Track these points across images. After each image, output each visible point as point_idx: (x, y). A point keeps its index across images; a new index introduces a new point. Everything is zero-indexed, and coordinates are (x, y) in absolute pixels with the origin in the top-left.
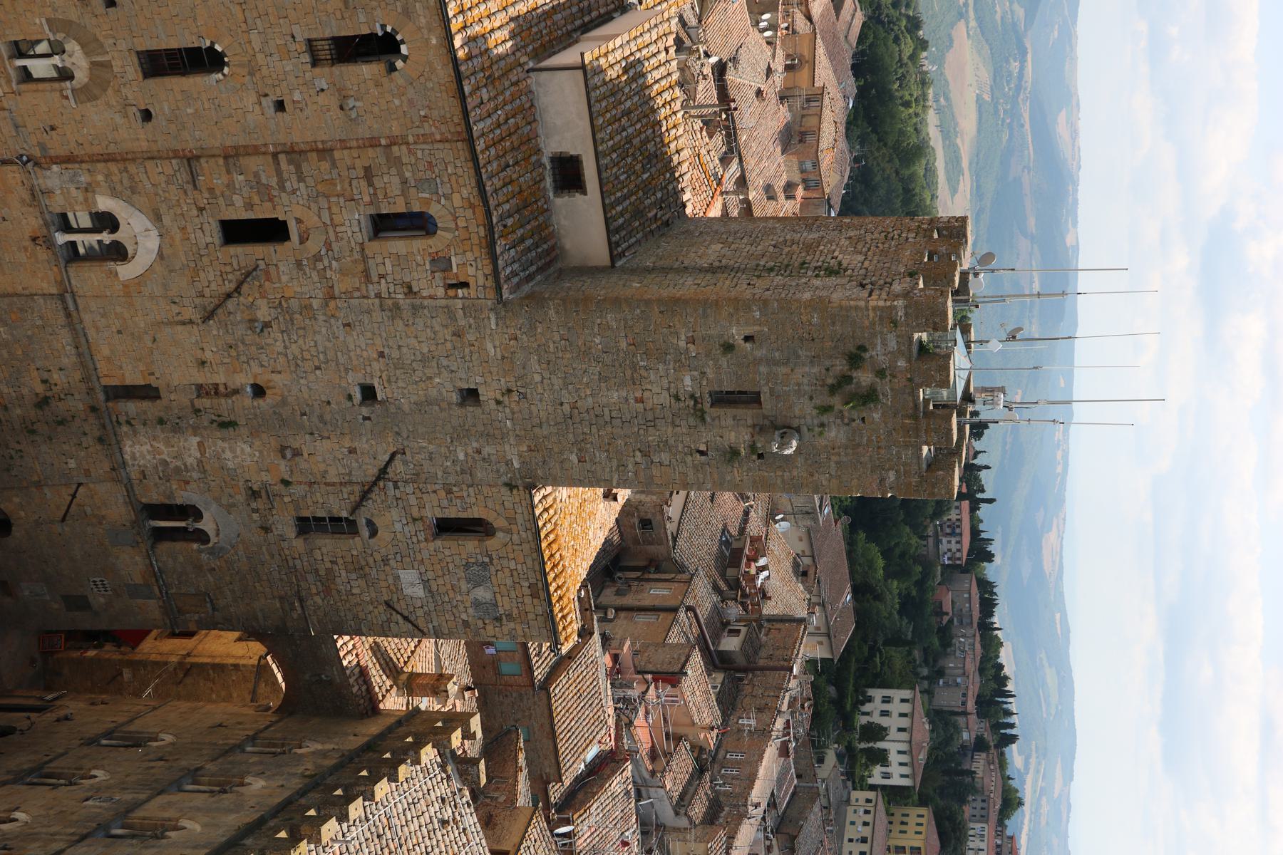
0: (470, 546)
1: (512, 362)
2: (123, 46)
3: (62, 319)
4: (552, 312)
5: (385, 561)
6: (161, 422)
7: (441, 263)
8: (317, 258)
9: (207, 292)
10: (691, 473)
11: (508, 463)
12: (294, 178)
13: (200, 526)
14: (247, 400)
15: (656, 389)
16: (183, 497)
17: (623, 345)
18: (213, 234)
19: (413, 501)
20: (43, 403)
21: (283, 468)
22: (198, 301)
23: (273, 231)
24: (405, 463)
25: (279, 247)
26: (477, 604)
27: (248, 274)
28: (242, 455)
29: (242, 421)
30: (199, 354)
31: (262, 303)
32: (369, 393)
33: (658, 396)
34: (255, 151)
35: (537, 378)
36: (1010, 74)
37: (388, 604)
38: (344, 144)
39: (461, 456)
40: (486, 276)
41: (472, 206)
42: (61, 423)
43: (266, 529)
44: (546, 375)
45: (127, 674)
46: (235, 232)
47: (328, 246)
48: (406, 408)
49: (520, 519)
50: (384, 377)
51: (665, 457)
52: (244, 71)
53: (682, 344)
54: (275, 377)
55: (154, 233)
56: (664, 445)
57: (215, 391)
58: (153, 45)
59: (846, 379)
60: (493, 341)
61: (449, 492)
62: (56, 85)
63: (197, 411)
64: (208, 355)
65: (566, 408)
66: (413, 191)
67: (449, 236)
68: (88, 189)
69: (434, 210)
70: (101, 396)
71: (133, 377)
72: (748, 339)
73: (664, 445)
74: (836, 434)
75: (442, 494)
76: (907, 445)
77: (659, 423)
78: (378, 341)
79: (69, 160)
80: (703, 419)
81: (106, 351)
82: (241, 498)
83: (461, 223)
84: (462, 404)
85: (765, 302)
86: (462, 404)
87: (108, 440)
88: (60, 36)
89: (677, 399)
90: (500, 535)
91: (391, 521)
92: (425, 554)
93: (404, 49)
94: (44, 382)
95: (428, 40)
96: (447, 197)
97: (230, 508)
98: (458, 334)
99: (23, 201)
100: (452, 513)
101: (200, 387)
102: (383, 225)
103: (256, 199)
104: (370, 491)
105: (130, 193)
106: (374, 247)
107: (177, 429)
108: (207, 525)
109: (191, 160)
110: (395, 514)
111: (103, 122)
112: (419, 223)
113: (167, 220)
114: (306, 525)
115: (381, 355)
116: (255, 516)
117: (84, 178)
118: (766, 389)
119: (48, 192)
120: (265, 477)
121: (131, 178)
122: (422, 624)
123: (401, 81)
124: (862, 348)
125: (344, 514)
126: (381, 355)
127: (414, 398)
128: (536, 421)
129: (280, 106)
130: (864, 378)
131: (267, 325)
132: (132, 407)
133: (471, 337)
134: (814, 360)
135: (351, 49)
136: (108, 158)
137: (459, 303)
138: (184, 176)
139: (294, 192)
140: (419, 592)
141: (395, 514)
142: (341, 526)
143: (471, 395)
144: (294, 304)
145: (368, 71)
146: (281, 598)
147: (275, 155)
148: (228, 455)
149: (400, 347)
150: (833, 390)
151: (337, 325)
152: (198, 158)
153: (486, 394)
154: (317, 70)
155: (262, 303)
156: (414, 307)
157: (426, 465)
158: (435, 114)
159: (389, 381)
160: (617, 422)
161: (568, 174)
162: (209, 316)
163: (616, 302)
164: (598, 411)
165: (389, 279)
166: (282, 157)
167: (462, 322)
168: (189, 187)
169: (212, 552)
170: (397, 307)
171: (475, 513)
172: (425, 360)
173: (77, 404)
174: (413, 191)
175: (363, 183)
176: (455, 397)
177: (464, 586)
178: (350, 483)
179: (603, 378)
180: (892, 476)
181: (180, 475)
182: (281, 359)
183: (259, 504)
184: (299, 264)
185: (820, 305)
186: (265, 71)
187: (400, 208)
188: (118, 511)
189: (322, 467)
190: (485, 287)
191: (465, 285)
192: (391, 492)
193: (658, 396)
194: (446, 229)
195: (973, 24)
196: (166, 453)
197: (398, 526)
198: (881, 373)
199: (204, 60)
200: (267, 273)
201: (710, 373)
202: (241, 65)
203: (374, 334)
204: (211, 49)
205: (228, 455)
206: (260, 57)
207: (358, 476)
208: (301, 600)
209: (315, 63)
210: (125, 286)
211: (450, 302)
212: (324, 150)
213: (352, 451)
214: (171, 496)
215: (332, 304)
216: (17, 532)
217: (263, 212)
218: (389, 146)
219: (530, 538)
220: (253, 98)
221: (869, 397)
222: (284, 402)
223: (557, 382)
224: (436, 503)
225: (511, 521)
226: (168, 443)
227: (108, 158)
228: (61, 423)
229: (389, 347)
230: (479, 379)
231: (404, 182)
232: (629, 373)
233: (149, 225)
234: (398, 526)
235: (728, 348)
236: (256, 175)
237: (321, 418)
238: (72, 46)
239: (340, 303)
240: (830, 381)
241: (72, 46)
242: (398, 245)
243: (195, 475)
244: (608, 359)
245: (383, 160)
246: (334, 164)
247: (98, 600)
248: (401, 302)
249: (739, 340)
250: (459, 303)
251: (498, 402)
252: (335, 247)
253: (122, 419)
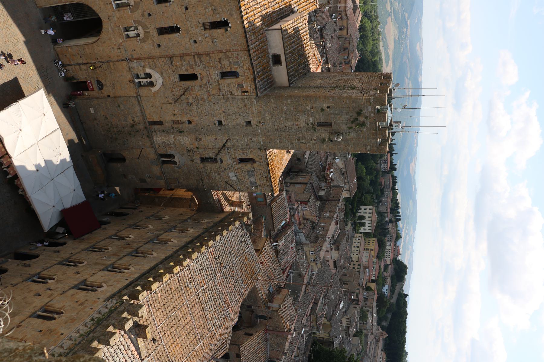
0: (249, 166)
2: (153, 27)
3: (137, 103)
4: (272, 99)
5: (225, 170)
6: (163, 131)
7: (240, 86)
8: (206, 84)
9: (175, 95)
10: (311, 146)
11: (260, 143)
12: (199, 62)
13: (174, 160)
14: (187, 124)
16: (170, 152)
17: (292, 109)
18: (177, 79)
19: (233, 153)
20: (133, 126)
21: (197, 144)
22: (173, 97)
23: (193, 77)
24: (231, 142)
25: (195, 82)
26: (251, 182)
27: (186, 90)
28: (185, 140)
29: (185, 131)
30: (173, 112)
31: (190, 97)
32: (220, 123)
33: (302, 124)
34: (188, 55)
35: (268, 118)
36: (403, 32)
37: (226, 182)
38: (213, 52)
39: (246, 141)
41: (249, 69)
42: (137, 131)
43: (192, 161)
45: (157, 200)
46: (183, 78)
47: (209, 81)
48: (231, 127)
49: (263, 159)
51: (304, 141)
52: (185, 32)
53: (309, 109)
54: (194, 118)
55: (161, 78)
56: (304, 138)
57: (178, 122)
58: (161, 26)
59: (356, 119)
61: (243, 151)
62: (135, 38)
63: (173, 128)
64: (176, 112)
65: (276, 127)
66: (232, 65)
67: (243, 78)
68: (144, 67)
69: (238, 70)
70: (148, 124)
71: (156, 119)
72: (328, 107)
73: (304, 138)
74: (353, 135)
75: (241, 151)
76: (373, 139)
77: (303, 131)
78: (223, 108)
79: (138, 59)
80: (315, 130)
81: (149, 112)
82: (185, 152)
83: (246, 74)
84: (246, 126)
85: (333, 97)
86: (246, 126)
87: (150, 136)
88: (137, 25)
89: (308, 124)
90: (257, 163)
91: (227, 159)
92: (236, 168)
93: (230, 25)
94: (133, 120)
95: (237, 22)
96: (242, 67)
97: (182, 155)
98: (245, 106)
99: (127, 71)
100: (243, 157)
101: (174, 121)
102: (224, 75)
103: (189, 68)
104: (220, 150)
105: (154, 68)
106: (222, 81)
107: (168, 133)
108: (176, 160)
109: (171, 58)
110: (228, 157)
111: (147, 48)
112: (234, 74)
113: (164, 75)
114: (203, 160)
115: (224, 112)
116: (189, 157)
117: (142, 64)
118: (333, 122)
119: (134, 68)
120: (192, 146)
121: (155, 63)
122: (235, 188)
123: (229, 34)
124: (361, 110)
125: (214, 157)
126: (224, 112)
127: (233, 124)
129: (195, 42)
130: (362, 119)
131: (192, 104)
132: (156, 127)
133: (249, 107)
134: (347, 114)
135: (215, 25)
136: (149, 58)
137: (246, 97)
138: (169, 62)
139: (199, 66)
140: (234, 178)
141: (228, 157)
142: (213, 160)
143: (249, 123)
144: (199, 97)
145: (220, 31)
146: (197, 180)
147: (194, 56)
148: (182, 140)
150: (352, 122)
151: (211, 103)
152: (173, 57)
153: (253, 123)
154: (206, 31)
155: (190, 97)
156: (233, 98)
158: (239, 43)
161: (277, 60)
162: (176, 101)
163: (291, 97)
164: (285, 128)
166: (196, 56)
168: (171, 65)
169: (178, 167)
170: (228, 98)
171: (250, 157)
172: (236, 113)
173: (141, 126)
174: (232, 65)
175: (218, 63)
176: (244, 124)
177: (247, 177)
178: (215, 148)
179: (286, 119)
180: (369, 147)
181: (168, 145)
182: (196, 113)
183: (190, 154)
184: (200, 86)
185: (349, 98)
186: (191, 32)
187: (229, 70)
188: (152, 155)
189: (207, 143)
191: (247, 92)
192: (227, 151)
193: (302, 124)
194: (242, 76)
195: (393, 17)
196: (165, 140)
197: (229, 160)
198: (366, 118)
199: (175, 30)
200: (192, 89)
202: (185, 31)
204: (176, 27)
205: (182, 140)
206: (190, 28)
207: (217, 146)
208: (202, 181)
209: (205, 29)
210: (154, 93)
212: (207, 54)
213: (216, 139)
214: (167, 151)
215: (210, 97)
216: (127, 161)
217: (190, 72)
218: (225, 52)
220: (188, 40)
221: (363, 124)
222: (197, 125)
223: (274, 120)
225: (260, 159)
226: (165, 137)
227: (149, 58)
228: (137, 131)
230: (251, 119)
231: (230, 63)
233: (160, 76)
234: (229, 160)
235: (323, 110)
236: (189, 61)
237: (207, 130)
238: (140, 27)
239: (212, 97)
240: (352, 120)
241: (140, 27)
242: (228, 81)
243: (173, 146)
244: (288, 113)
245: (224, 56)
246: (210, 58)
247: (148, 180)
249: (326, 108)
250: (246, 97)
251: (257, 125)
252: (211, 81)
253: (153, 130)
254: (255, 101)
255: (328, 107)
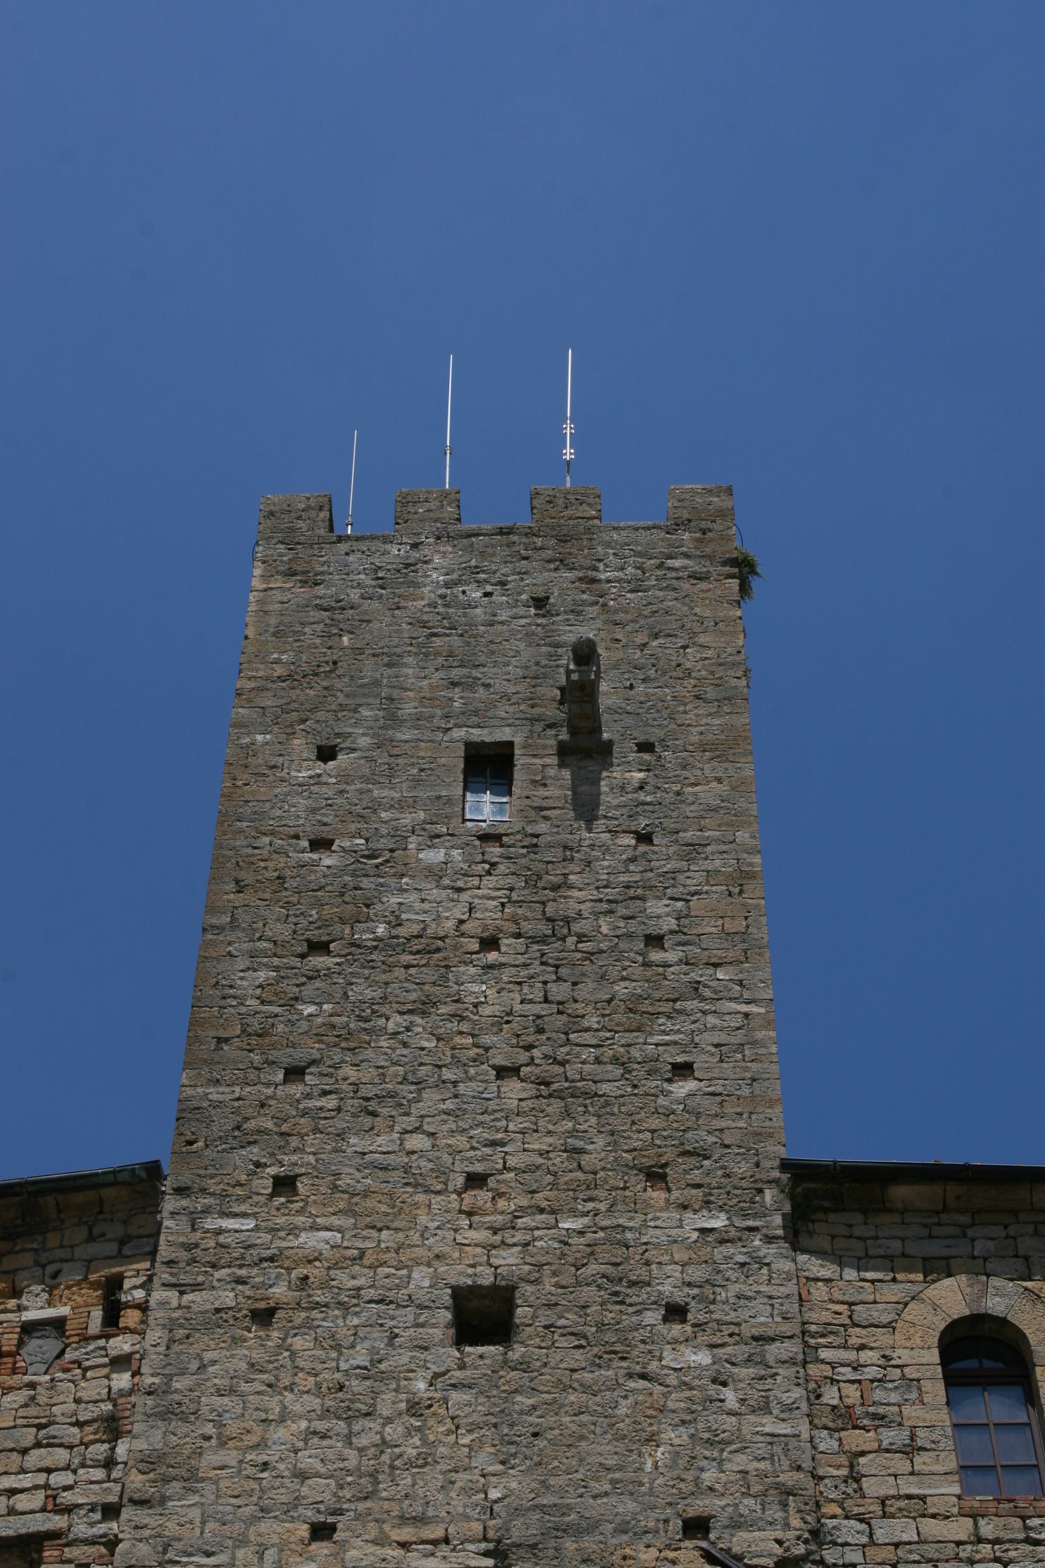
1: (366, 1194)
4: (215, 1094)
15: (459, 911)
35: (416, 1142)
39: (703, 1358)
40: (91, 1239)
44: (410, 1122)
50: (406, 1533)
60: (293, 1231)
61: (845, 1418)
75: (855, 1439)
118: (459, 733)
126: (321, 1532)
127: (484, 1460)
128: (558, 1159)
133: (280, 1291)
143: (483, 1317)
149: (302, 1476)
156: (165, 1415)
157: (741, 1461)
159: (420, 1520)
160: (559, 991)
165: (59, 1479)
167: (227, 1297)
190: (122, 1242)
201: (407, 819)
203: (242, 1541)
211: (157, 1315)
219: (998, 1232)
224: (900, 1464)
229: (297, 1501)
230: (421, 1277)
232: (407, 958)
248: (141, 1444)
254: (212, 1223)
255: (326, 754)
